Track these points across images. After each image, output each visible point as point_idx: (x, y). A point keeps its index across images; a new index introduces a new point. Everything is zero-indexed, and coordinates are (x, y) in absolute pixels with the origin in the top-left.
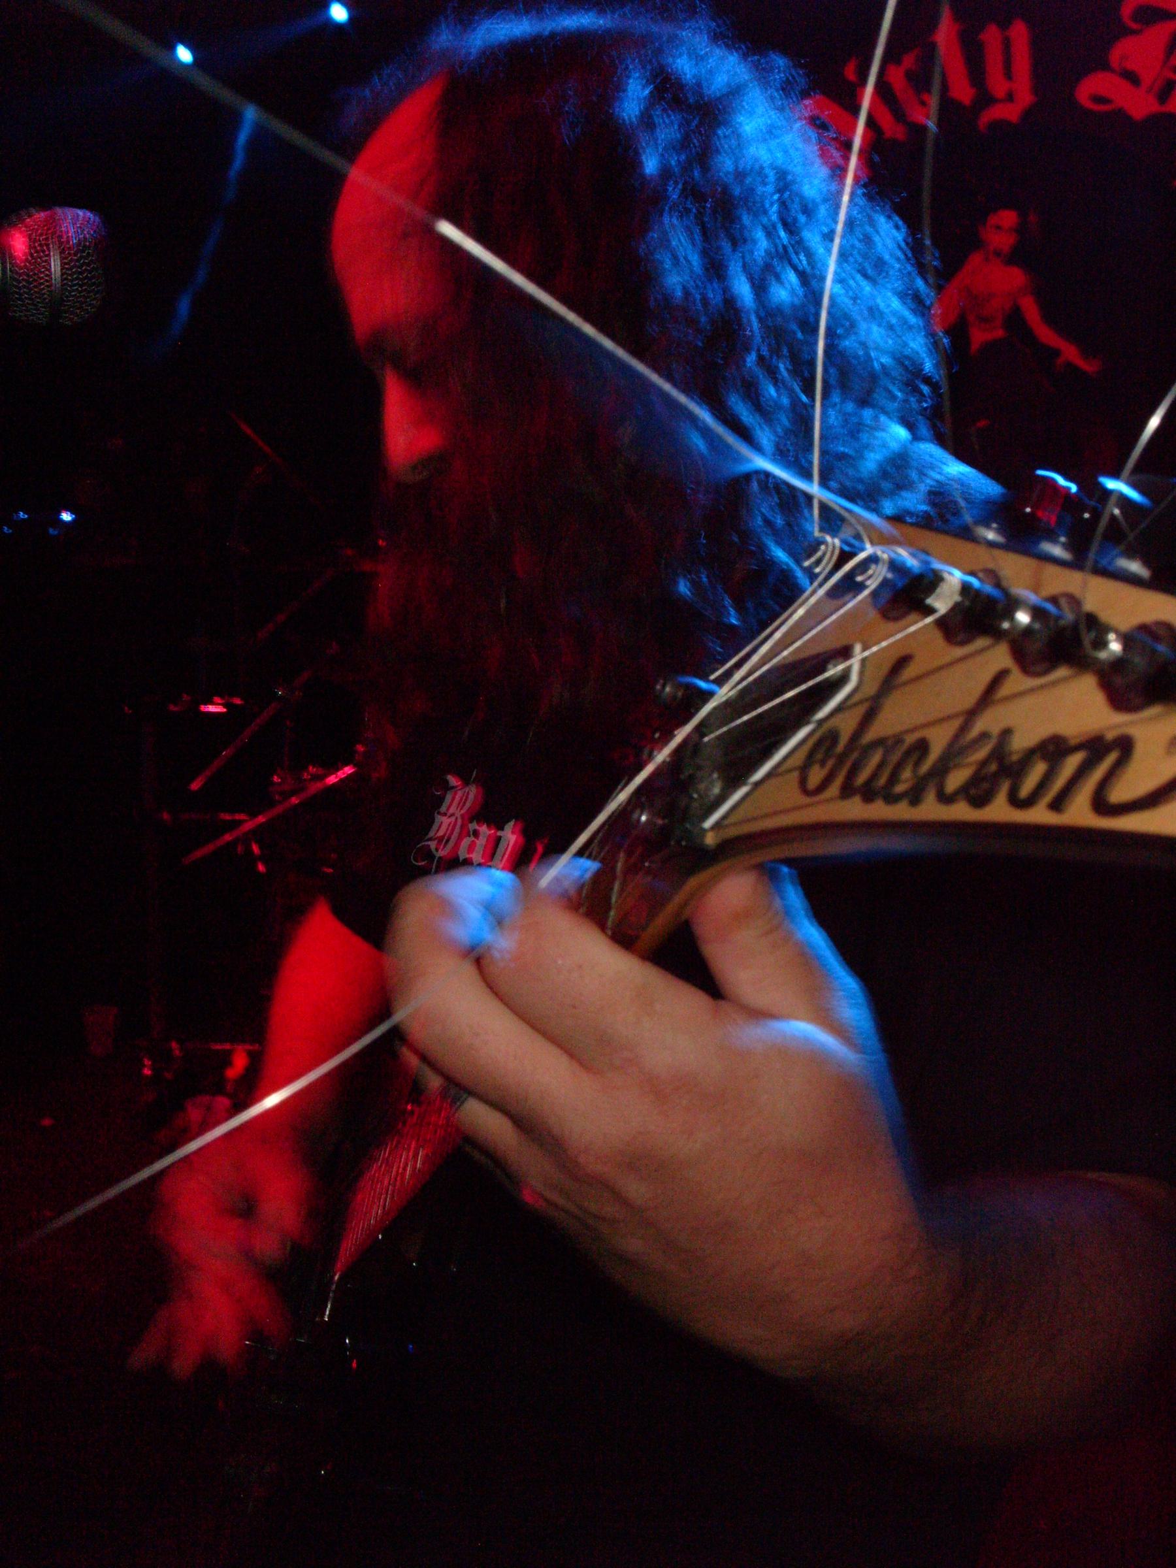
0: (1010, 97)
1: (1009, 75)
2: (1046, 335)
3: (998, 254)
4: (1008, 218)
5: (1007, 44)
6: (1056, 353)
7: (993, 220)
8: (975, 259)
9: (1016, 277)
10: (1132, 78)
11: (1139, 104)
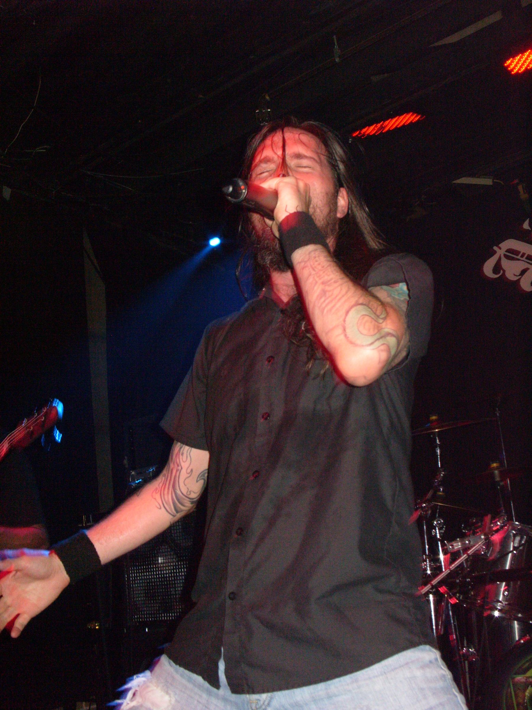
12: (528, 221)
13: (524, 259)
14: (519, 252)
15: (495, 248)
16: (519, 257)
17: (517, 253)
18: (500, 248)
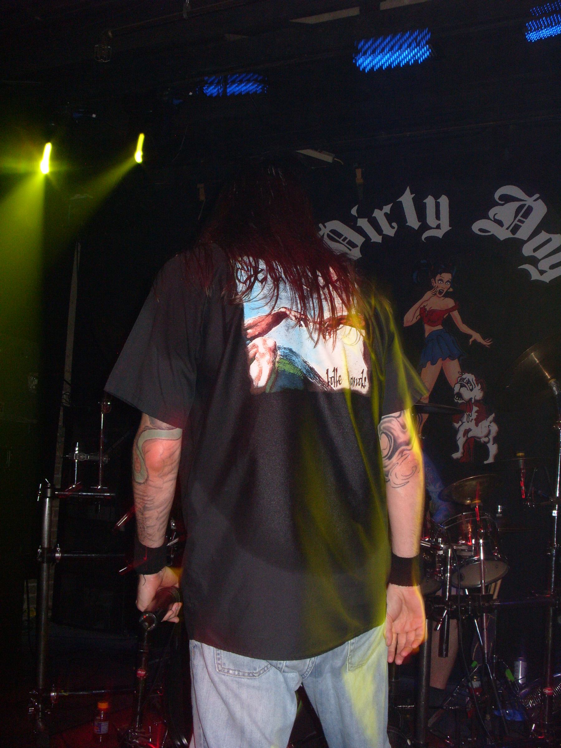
0: (438, 227)
1: (438, 217)
2: (464, 328)
3: (440, 293)
4: (447, 276)
5: (438, 205)
6: (471, 336)
7: (438, 277)
8: (428, 294)
9: (450, 303)
10: (500, 223)
11: (503, 234)
12: (355, 208)
13: (345, 243)
14: (343, 235)
15: (321, 225)
16: (340, 240)
17: (339, 235)
18: (325, 227)
